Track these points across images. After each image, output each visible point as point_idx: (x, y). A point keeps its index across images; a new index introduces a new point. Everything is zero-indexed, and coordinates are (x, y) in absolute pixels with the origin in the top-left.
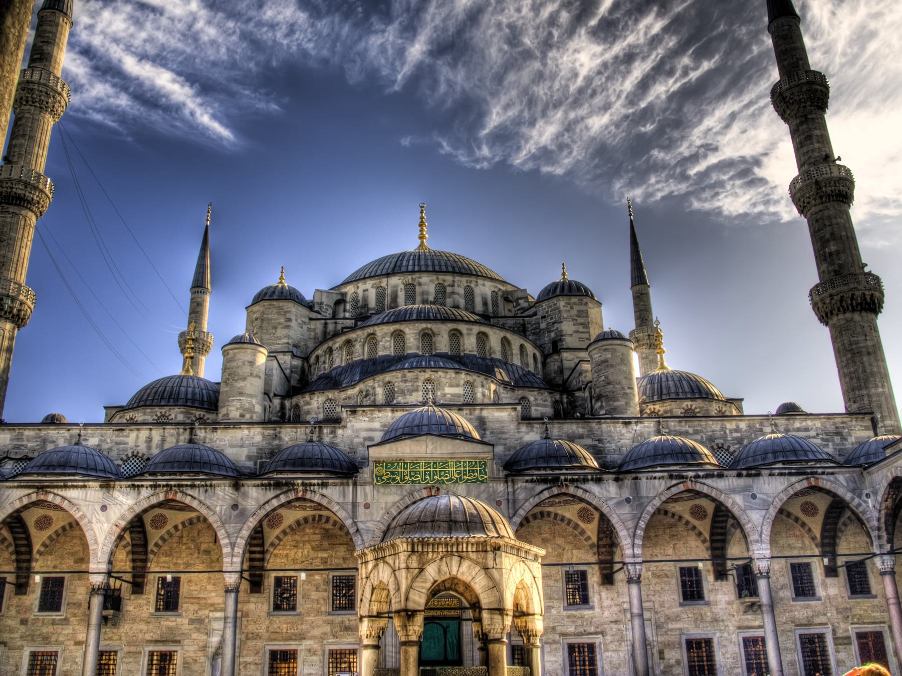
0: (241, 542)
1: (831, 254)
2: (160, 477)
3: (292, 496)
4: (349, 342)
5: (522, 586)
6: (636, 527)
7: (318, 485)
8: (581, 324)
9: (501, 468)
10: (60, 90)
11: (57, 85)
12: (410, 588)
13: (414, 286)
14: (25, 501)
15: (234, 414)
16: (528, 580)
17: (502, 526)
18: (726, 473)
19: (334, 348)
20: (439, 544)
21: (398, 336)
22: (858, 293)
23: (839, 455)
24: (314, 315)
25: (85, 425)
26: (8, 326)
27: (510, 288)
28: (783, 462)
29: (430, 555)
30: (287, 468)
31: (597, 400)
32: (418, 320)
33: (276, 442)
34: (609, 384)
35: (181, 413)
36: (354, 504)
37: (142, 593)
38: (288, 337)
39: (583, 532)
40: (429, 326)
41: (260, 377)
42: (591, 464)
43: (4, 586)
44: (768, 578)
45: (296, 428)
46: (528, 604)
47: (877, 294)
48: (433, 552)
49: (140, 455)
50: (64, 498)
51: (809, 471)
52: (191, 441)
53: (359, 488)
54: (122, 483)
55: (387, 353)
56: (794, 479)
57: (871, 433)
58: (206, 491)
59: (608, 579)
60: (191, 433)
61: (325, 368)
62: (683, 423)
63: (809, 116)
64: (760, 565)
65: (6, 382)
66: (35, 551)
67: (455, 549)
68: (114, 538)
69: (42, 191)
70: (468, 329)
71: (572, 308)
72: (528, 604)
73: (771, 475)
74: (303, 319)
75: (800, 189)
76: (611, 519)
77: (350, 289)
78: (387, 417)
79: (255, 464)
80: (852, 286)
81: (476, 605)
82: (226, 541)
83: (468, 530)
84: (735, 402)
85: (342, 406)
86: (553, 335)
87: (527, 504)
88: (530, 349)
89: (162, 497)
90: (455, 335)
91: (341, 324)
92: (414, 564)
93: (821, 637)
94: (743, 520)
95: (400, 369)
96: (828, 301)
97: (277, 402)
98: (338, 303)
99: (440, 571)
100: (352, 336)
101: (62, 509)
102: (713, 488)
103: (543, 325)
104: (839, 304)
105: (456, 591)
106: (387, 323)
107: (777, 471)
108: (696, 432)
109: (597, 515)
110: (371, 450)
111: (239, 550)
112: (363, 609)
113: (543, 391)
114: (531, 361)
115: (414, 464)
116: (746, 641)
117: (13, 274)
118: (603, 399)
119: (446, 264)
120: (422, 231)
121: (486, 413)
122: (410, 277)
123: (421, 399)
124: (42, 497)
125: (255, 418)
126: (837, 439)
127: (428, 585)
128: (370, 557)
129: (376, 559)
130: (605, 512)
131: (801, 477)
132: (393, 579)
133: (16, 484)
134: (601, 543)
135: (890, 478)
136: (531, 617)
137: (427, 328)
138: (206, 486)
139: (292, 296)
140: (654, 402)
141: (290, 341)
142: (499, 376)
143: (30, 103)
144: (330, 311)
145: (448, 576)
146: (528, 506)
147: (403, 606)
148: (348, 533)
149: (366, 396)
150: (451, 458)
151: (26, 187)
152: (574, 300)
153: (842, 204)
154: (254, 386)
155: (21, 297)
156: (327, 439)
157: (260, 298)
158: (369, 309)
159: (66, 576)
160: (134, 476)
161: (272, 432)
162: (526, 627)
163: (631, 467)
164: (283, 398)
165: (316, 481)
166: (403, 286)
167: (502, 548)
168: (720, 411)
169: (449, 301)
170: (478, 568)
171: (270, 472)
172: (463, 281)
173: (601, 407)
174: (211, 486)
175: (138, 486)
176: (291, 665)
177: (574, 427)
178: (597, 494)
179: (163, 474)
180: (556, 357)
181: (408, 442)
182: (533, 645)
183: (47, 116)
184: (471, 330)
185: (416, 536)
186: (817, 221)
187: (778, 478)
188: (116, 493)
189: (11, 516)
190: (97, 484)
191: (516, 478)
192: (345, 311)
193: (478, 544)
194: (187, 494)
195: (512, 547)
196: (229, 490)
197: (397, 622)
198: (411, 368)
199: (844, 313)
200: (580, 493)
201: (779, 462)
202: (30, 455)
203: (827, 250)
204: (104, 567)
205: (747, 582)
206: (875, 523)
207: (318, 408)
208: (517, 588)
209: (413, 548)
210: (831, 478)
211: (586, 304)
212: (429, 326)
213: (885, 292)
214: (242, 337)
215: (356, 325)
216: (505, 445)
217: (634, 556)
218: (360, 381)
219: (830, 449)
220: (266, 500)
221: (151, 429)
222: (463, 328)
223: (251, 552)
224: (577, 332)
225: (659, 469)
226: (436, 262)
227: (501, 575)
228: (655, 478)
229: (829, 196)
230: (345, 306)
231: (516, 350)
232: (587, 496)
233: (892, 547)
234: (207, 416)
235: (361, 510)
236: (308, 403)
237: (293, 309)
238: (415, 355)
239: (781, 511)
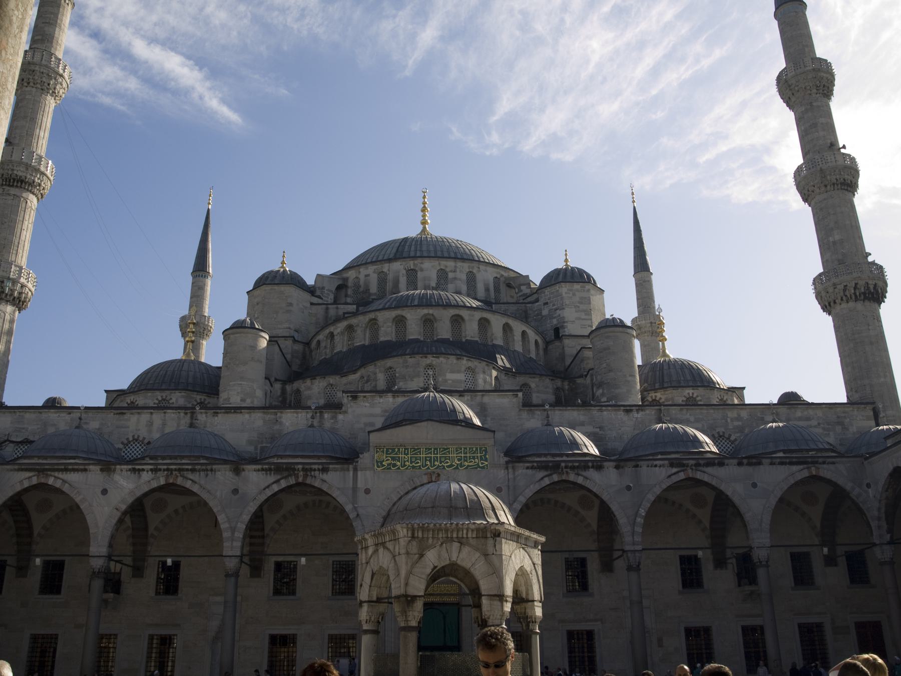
0: (242, 527)
1: (834, 243)
2: (160, 461)
3: (292, 481)
5: (521, 573)
6: (637, 514)
7: (319, 470)
8: (584, 311)
9: (502, 455)
10: (61, 71)
11: (58, 67)
12: (410, 573)
14: (26, 484)
16: (528, 566)
17: (502, 513)
18: (726, 461)
19: (335, 333)
20: (440, 530)
21: (400, 322)
22: (861, 283)
23: (841, 445)
24: (315, 300)
25: (86, 408)
26: (9, 308)
27: (512, 275)
28: (784, 451)
29: (430, 541)
30: (288, 453)
31: (598, 388)
32: (419, 306)
33: (277, 427)
34: (610, 371)
35: (183, 397)
36: (355, 489)
37: (142, 577)
40: (431, 311)
42: (713, 450)
43: (4, 569)
44: (767, 566)
45: (297, 413)
46: (527, 590)
47: (880, 284)
48: (433, 538)
49: (141, 439)
50: (64, 481)
51: (810, 460)
52: (191, 425)
53: (359, 473)
54: (123, 467)
55: (388, 338)
56: (795, 468)
57: (873, 423)
58: (207, 475)
59: (607, 567)
60: (192, 418)
61: (324, 353)
62: (685, 411)
63: (814, 104)
64: (760, 554)
65: (6, 365)
66: (36, 532)
67: (455, 535)
68: (114, 521)
69: (43, 174)
71: (574, 295)
72: (527, 590)
73: (771, 464)
75: (805, 177)
76: (611, 506)
77: (351, 274)
78: (390, 402)
79: (256, 448)
80: (855, 275)
81: (476, 592)
82: (227, 525)
83: (469, 517)
84: (738, 391)
85: (343, 392)
86: (555, 321)
87: (527, 491)
88: (532, 335)
89: (162, 482)
90: (457, 321)
91: (343, 308)
92: (414, 548)
93: (819, 626)
94: (743, 509)
95: (401, 355)
96: (831, 290)
97: (278, 386)
98: (342, 287)
99: (439, 556)
100: (354, 321)
101: (63, 493)
102: (713, 476)
103: (545, 312)
104: (842, 294)
105: (456, 577)
106: (390, 308)
107: (778, 460)
108: (697, 420)
109: (597, 503)
110: (372, 435)
111: (239, 535)
112: (363, 594)
113: (544, 378)
114: (532, 347)
115: (415, 450)
116: (744, 629)
117: (14, 256)
120: (424, 216)
121: (487, 399)
122: (412, 262)
123: (422, 385)
124: (43, 480)
125: (256, 403)
126: (839, 429)
127: (428, 571)
128: (370, 542)
129: (376, 545)
131: (802, 467)
133: (16, 467)
135: (891, 468)
137: (428, 314)
139: (294, 280)
140: (655, 390)
141: (292, 327)
142: (500, 363)
143: (31, 84)
144: (332, 296)
145: (448, 562)
146: (529, 493)
147: (402, 591)
148: (348, 518)
149: (367, 381)
150: (452, 444)
151: (27, 169)
152: (577, 286)
153: (846, 193)
154: (257, 371)
155: (22, 280)
156: (328, 424)
157: (262, 282)
158: (370, 294)
159: (67, 559)
160: (135, 460)
161: (273, 417)
162: (525, 613)
163: (631, 455)
164: (284, 383)
165: (316, 467)
166: (404, 272)
168: (721, 400)
169: (451, 286)
170: (478, 555)
171: (272, 457)
172: (465, 267)
173: (603, 395)
174: (212, 470)
175: (139, 470)
176: (291, 650)
177: (575, 413)
179: (163, 458)
180: (557, 343)
181: (409, 428)
182: (532, 631)
183: (49, 97)
184: (473, 316)
185: (417, 522)
186: (821, 209)
187: (779, 467)
188: (117, 477)
189: (11, 498)
190: (98, 468)
191: (517, 464)
192: (346, 296)
193: (478, 530)
194: (187, 479)
195: (513, 533)
196: (230, 475)
197: (397, 607)
198: (413, 354)
200: (580, 480)
201: (780, 451)
202: (31, 438)
203: (831, 239)
204: (104, 551)
205: (747, 570)
206: (876, 513)
207: (319, 393)
209: (413, 534)
210: (832, 467)
211: (589, 290)
212: (431, 311)
213: (888, 282)
214: (244, 321)
215: (357, 309)
217: (634, 544)
218: (360, 367)
219: (831, 440)
220: (266, 485)
221: (151, 413)
223: (251, 537)
224: (579, 319)
225: (659, 457)
226: (438, 248)
228: (656, 466)
229: (834, 184)
230: (346, 291)
231: (518, 337)
232: (588, 484)
233: (891, 537)
234: (208, 400)
235: (361, 494)
236: (309, 388)
238: (416, 341)
239: (781, 500)
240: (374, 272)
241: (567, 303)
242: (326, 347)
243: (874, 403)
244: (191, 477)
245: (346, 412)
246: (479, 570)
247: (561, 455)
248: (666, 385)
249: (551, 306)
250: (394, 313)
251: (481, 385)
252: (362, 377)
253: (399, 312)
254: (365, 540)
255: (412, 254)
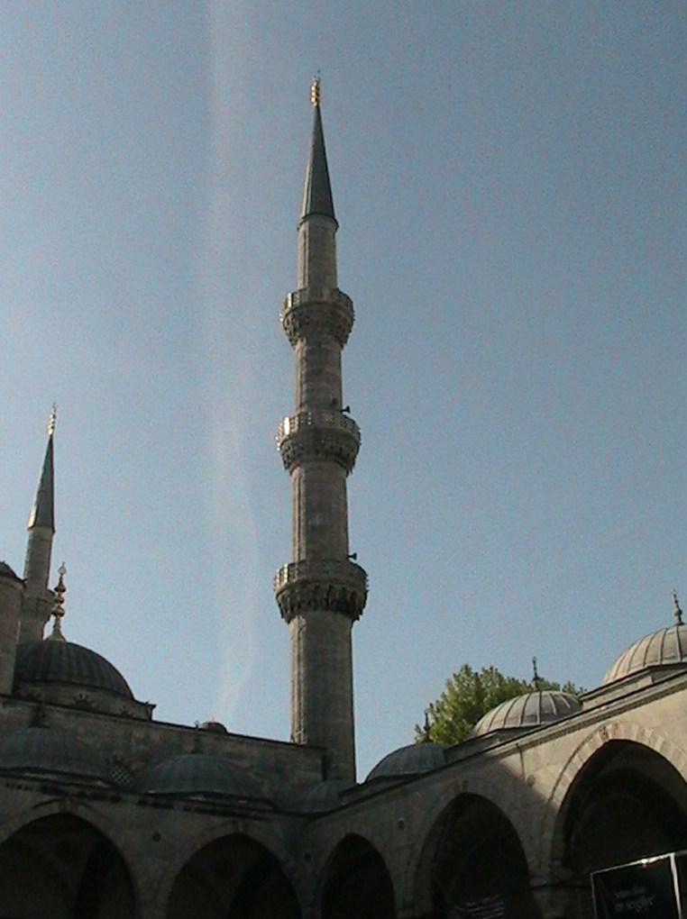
22: (338, 587)
47: (360, 594)
56: (217, 820)
57: (319, 776)
62: (72, 717)
73: (186, 809)
107: (196, 806)
131: (227, 819)
135: (343, 835)
140: (35, 682)
153: (339, 466)
199: (315, 609)
219: (266, 790)
225: (27, 774)
228: (20, 787)
243: (326, 749)
248: (51, 676)
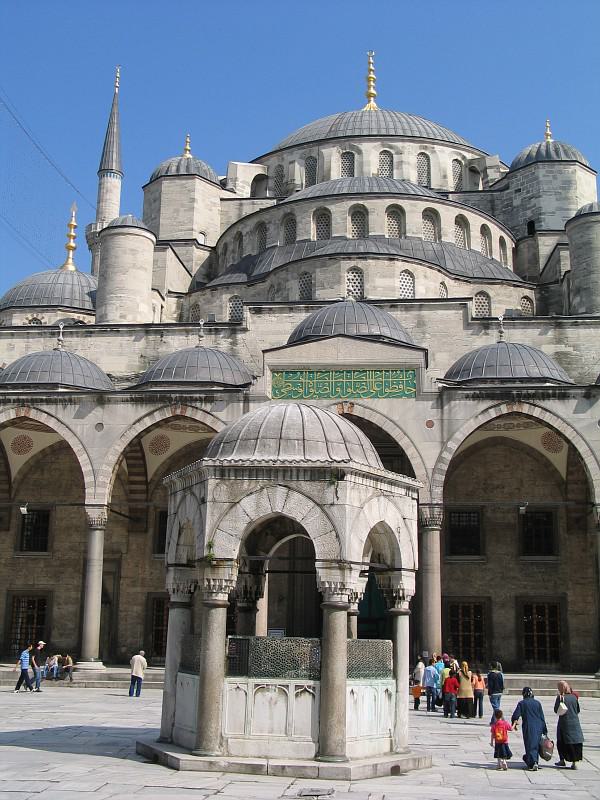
3: (168, 414)
4: (262, 227)
7: (201, 400)
13: (353, 155)
15: (114, 317)
19: (244, 233)
29: (246, 485)
31: (575, 295)
34: (591, 272)
38: (191, 221)
39: (548, 464)
41: (146, 269)
46: (393, 555)
53: (251, 405)
70: (411, 205)
71: (555, 178)
72: (393, 555)
74: (213, 200)
85: (247, 304)
86: (529, 213)
88: (496, 232)
89: (12, 415)
97: (172, 302)
100: (265, 217)
103: (517, 202)
110: (266, 355)
112: (170, 558)
118: (583, 293)
119: (395, 126)
120: (369, 87)
121: (424, 313)
130: (570, 438)
132: (198, 516)
134: (570, 477)
136: (396, 572)
138: (65, 401)
141: (195, 227)
167: (348, 477)
178: (560, 413)
179: (15, 386)
180: (530, 241)
200: (537, 413)
208: (374, 531)
212: (361, 202)
216: (450, 351)
222: (404, 203)
227: (343, 516)
231: (475, 231)
232: (547, 417)
237: (199, 185)
238: (344, 238)
240: (301, 158)
241: (546, 188)
242: (233, 251)
244: (47, 410)
245: (245, 330)
246: (313, 524)
247: (513, 380)
249: (524, 194)
250: (314, 206)
251: (421, 293)
252: (272, 286)
253: (320, 204)
254: (175, 483)
255: (349, 133)
